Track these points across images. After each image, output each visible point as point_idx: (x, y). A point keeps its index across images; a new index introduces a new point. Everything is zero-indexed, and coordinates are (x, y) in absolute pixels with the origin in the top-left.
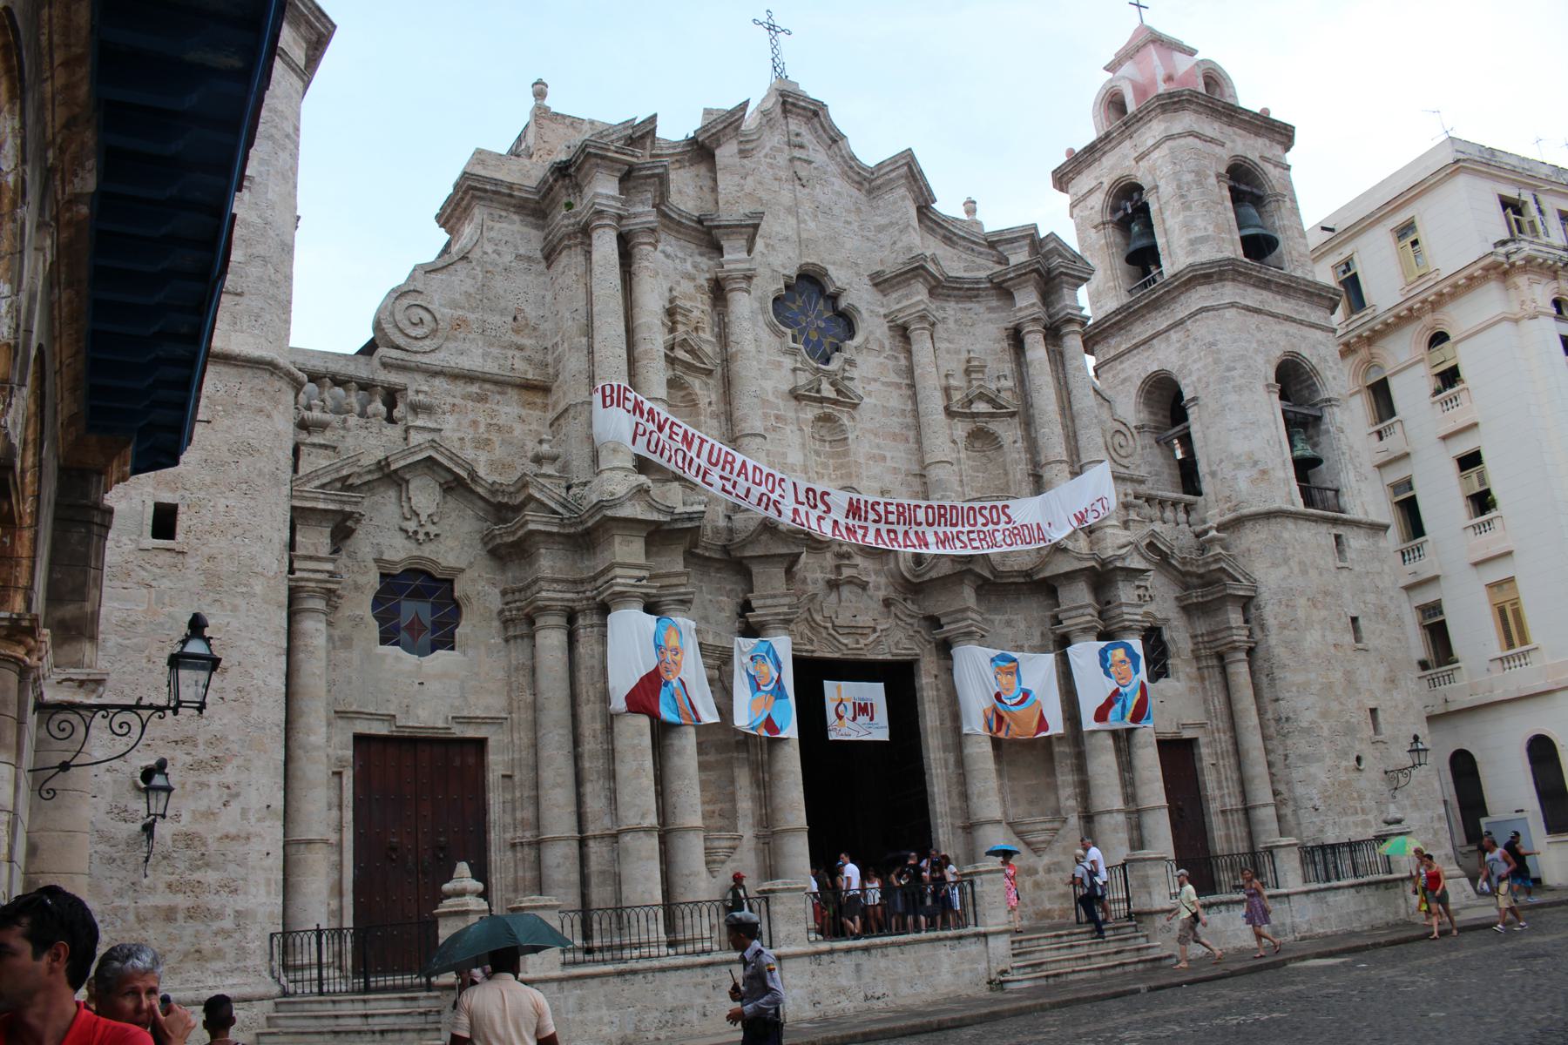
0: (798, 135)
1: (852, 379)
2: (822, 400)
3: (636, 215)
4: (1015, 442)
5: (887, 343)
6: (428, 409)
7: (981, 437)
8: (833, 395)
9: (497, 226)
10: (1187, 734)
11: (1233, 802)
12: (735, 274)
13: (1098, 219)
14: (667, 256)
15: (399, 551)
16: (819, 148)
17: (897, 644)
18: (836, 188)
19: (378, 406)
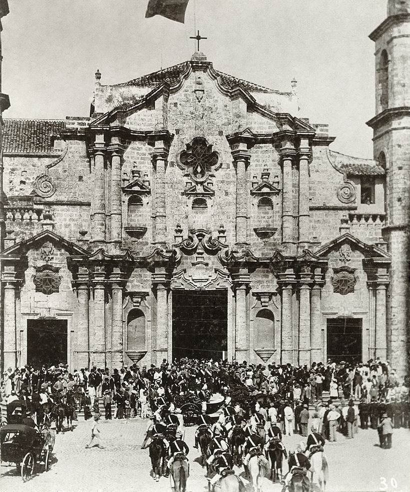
0: (199, 78)
1: (212, 184)
2: (197, 194)
3: (113, 145)
4: (278, 204)
5: (231, 165)
6: (49, 217)
7: (266, 202)
8: (203, 192)
9: (73, 146)
10: (355, 317)
11: (372, 345)
12: (157, 154)
13: (378, 67)
14: (134, 149)
15: (41, 263)
16: (210, 81)
17: (218, 285)
18: (215, 98)
19: (35, 216)
